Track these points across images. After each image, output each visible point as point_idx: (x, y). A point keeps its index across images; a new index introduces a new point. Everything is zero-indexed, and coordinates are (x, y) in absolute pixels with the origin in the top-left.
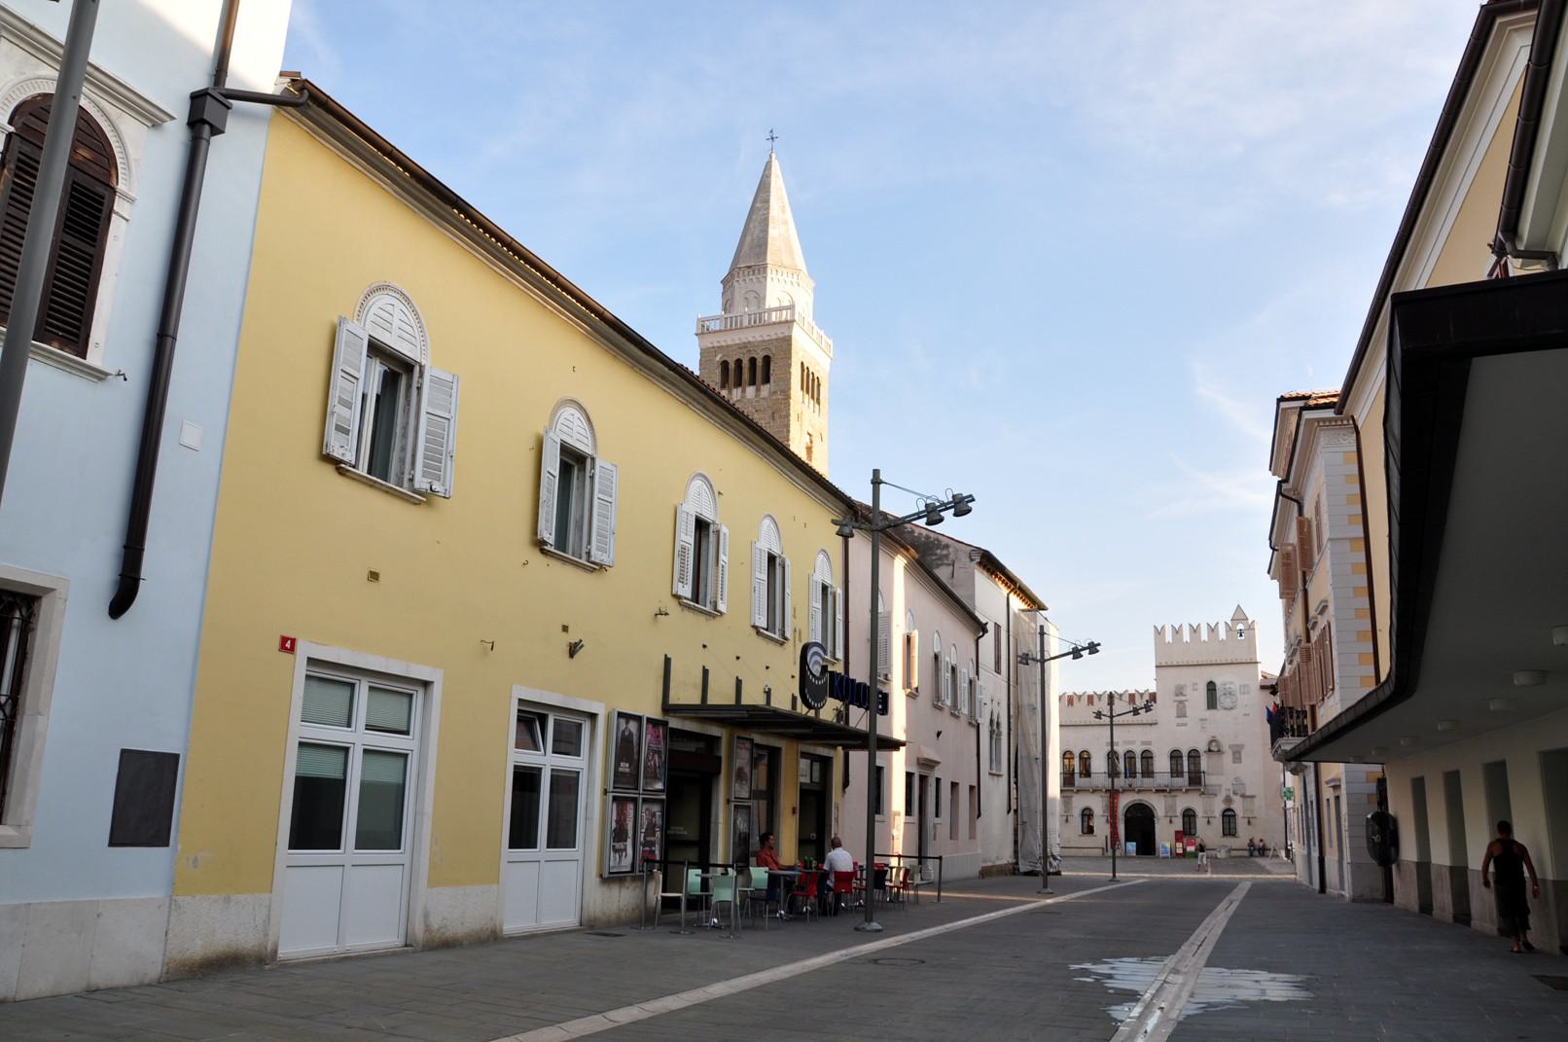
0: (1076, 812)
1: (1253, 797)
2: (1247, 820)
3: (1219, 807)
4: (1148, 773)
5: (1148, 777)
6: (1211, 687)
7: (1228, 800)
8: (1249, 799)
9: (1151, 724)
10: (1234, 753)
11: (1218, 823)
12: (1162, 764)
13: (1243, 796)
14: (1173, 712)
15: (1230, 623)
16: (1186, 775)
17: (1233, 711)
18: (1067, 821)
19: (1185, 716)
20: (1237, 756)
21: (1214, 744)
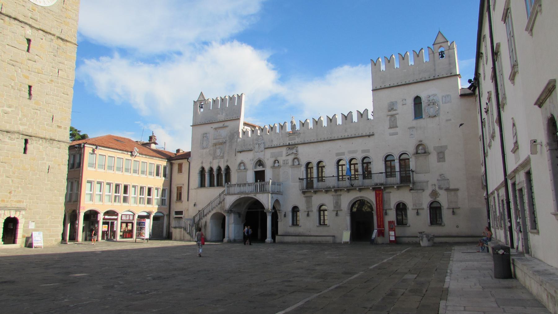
0: (315, 209)
1: (457, 190)
2: (451, 210)
3: (426, 200)
4: (367, 174)
5: (368, 178)
6: (417, 101)
7: (434, 194)
8: (453, 193)
9: (369, 136)
10: (438, 153)
11: (426, 215)
12: (378, 167)
13: (448, 190)
14: (387, 124)
15: (432, 47)
16: (398, 174)
17: (437, 118)
18: (308, 215)
19: (397, 127)
20: (441, 156)
21: (421, 147)
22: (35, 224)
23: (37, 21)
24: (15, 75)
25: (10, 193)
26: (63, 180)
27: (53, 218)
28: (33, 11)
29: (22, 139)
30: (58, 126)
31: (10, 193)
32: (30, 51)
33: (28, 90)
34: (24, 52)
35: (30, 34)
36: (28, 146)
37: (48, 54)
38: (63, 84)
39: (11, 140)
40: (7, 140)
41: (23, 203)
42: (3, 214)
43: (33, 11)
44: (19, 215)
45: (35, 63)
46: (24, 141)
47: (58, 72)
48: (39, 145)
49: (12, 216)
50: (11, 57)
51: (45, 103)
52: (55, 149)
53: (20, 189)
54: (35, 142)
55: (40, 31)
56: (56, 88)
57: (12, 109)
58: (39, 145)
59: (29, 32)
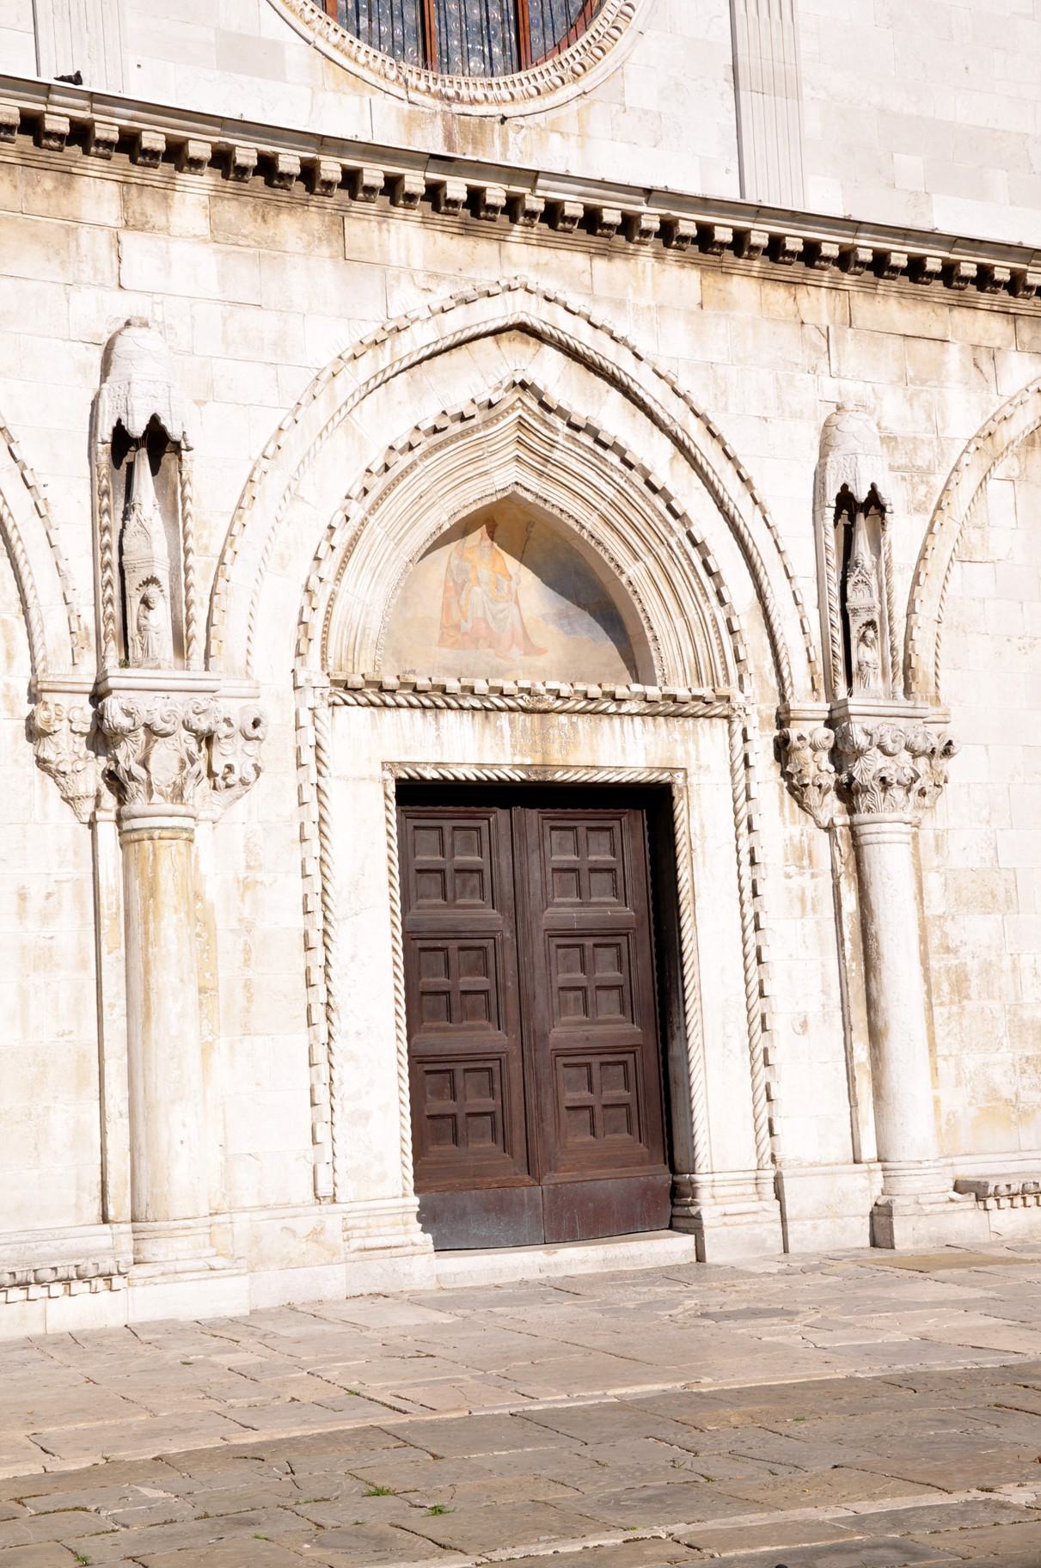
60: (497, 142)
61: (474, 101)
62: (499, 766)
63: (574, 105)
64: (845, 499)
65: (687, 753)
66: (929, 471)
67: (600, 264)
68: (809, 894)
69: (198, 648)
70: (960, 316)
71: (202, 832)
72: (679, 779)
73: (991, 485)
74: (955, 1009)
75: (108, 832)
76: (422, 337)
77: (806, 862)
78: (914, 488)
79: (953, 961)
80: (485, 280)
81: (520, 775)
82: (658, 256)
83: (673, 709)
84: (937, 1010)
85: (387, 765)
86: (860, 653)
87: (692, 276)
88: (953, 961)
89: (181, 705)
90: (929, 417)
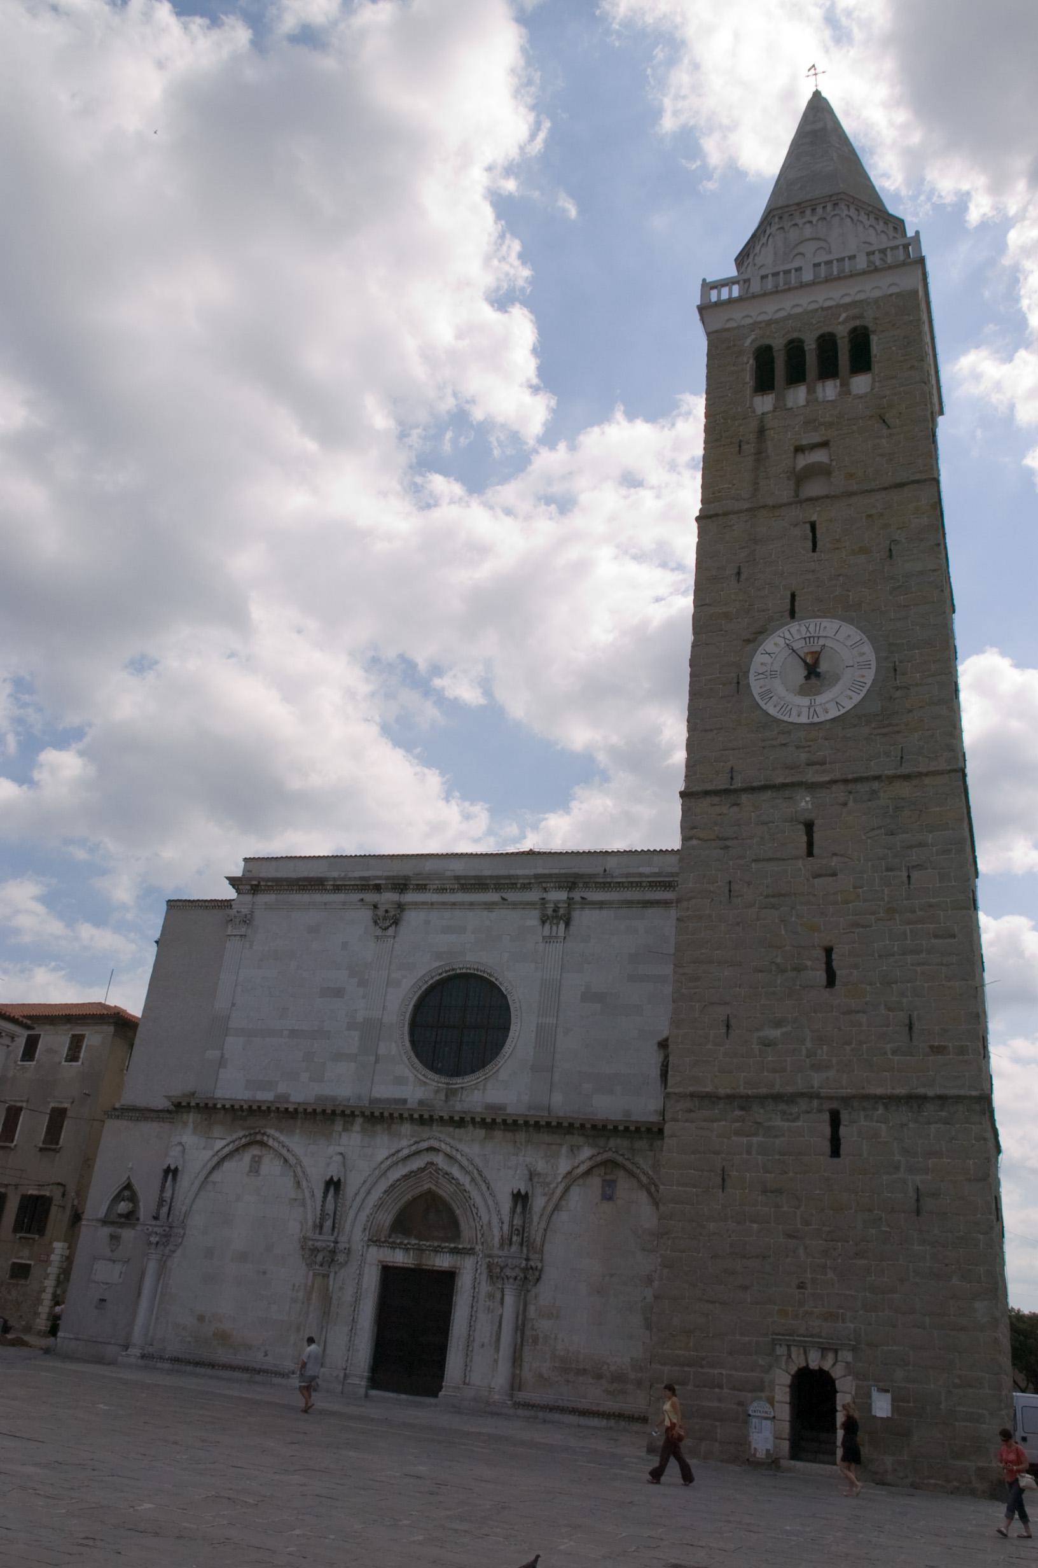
22: (893, 1400)
23: (823, 763)
24: (783, 932)
25: (801, 1286)
26: (981, 1237)
27: (957, 1381)
28: (809, 743)
29: (820, 1111)
30: (932, 1047)
31: (801, 1286)
32: (816, 851)
33: (824, 960)
34: (800, 863)
35: (810, 806)
36: (843, 1131)
37: (870, 838)
38: (930, 906)
39: (788, 1120)
40: (778, 1123)
41: (844, 1321)
42: (784, 1358)
43: (809, 743)
44: (834, 1364)
45: (834, 878)
46: (826, 1116)
47: (909, 877)
48: (877, 1122)
49: (814, 1365)
50: (767, 887)
51: (878, 985)
52: (932, 1126)
53: (830, 1274)
54: (862, 1114)
55: (834, 787)
56: (908, 927)
57: (784, 1029)
58: (875, 1124)
59: (807, 802)
60: (460, 1094)
61: (456, 1084)
62: (408, 1264)
63: (483, 1082)
64: (513, 1192)
65: (461, 1263)
66: (548, 1184)
67: (457, 1130)
68: (491, 1307)
69: (336, 1230)
70: (567, 1136)
71: (332, 1275)
72: (457, 1271)
73: (573, 1188)
74: (533, 1348)
75: (311, 1273)
76: (406, 1152)
77: (492, 1298)
78: (544, 1189)
79: (534, 1333)
80: (425, 1136)
81: (413, 1266)
82: (474, 1127)
83: (455, 1251)
84: (526, 1348)
85: (380, 1261)
86: (515, 1238)
87: (481, 1133)
88: (534, 1333)
89: (324, 1245)
90: (553, 1167)
